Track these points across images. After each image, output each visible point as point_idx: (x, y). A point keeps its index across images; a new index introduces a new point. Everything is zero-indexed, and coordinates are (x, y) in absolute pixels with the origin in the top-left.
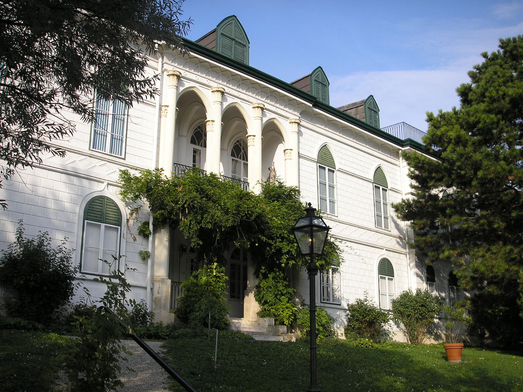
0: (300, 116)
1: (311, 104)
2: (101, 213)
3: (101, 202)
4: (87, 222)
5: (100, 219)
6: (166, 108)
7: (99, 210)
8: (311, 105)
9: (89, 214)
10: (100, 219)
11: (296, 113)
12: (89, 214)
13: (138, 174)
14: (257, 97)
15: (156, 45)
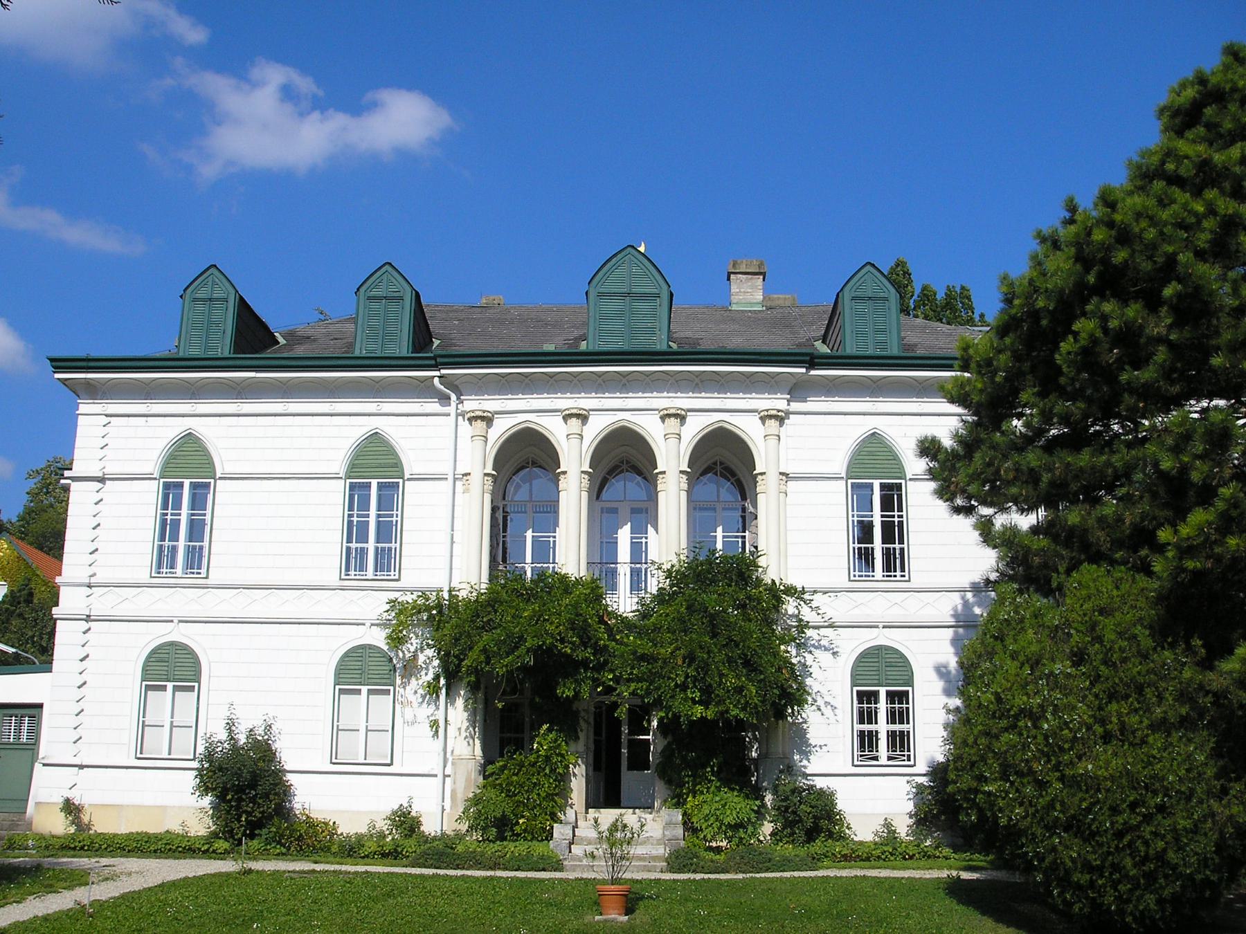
0: (789, 396)
1: (803, 367)
2: (360, 672)
3: (360, 655)
4: (340, 689)
5: (359, 680)
6: (468, 477)
7: (357, 667)
8: (804, 370)
9: (341, 676)
10: (359, 680)
11: (779, 395)
12: (341, 676)
13: (409, 598)
14: (670, 395)
15: (436, 380)
